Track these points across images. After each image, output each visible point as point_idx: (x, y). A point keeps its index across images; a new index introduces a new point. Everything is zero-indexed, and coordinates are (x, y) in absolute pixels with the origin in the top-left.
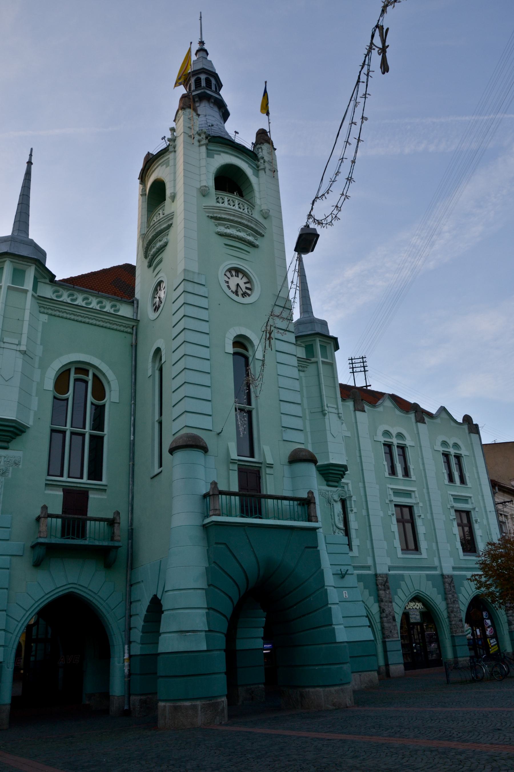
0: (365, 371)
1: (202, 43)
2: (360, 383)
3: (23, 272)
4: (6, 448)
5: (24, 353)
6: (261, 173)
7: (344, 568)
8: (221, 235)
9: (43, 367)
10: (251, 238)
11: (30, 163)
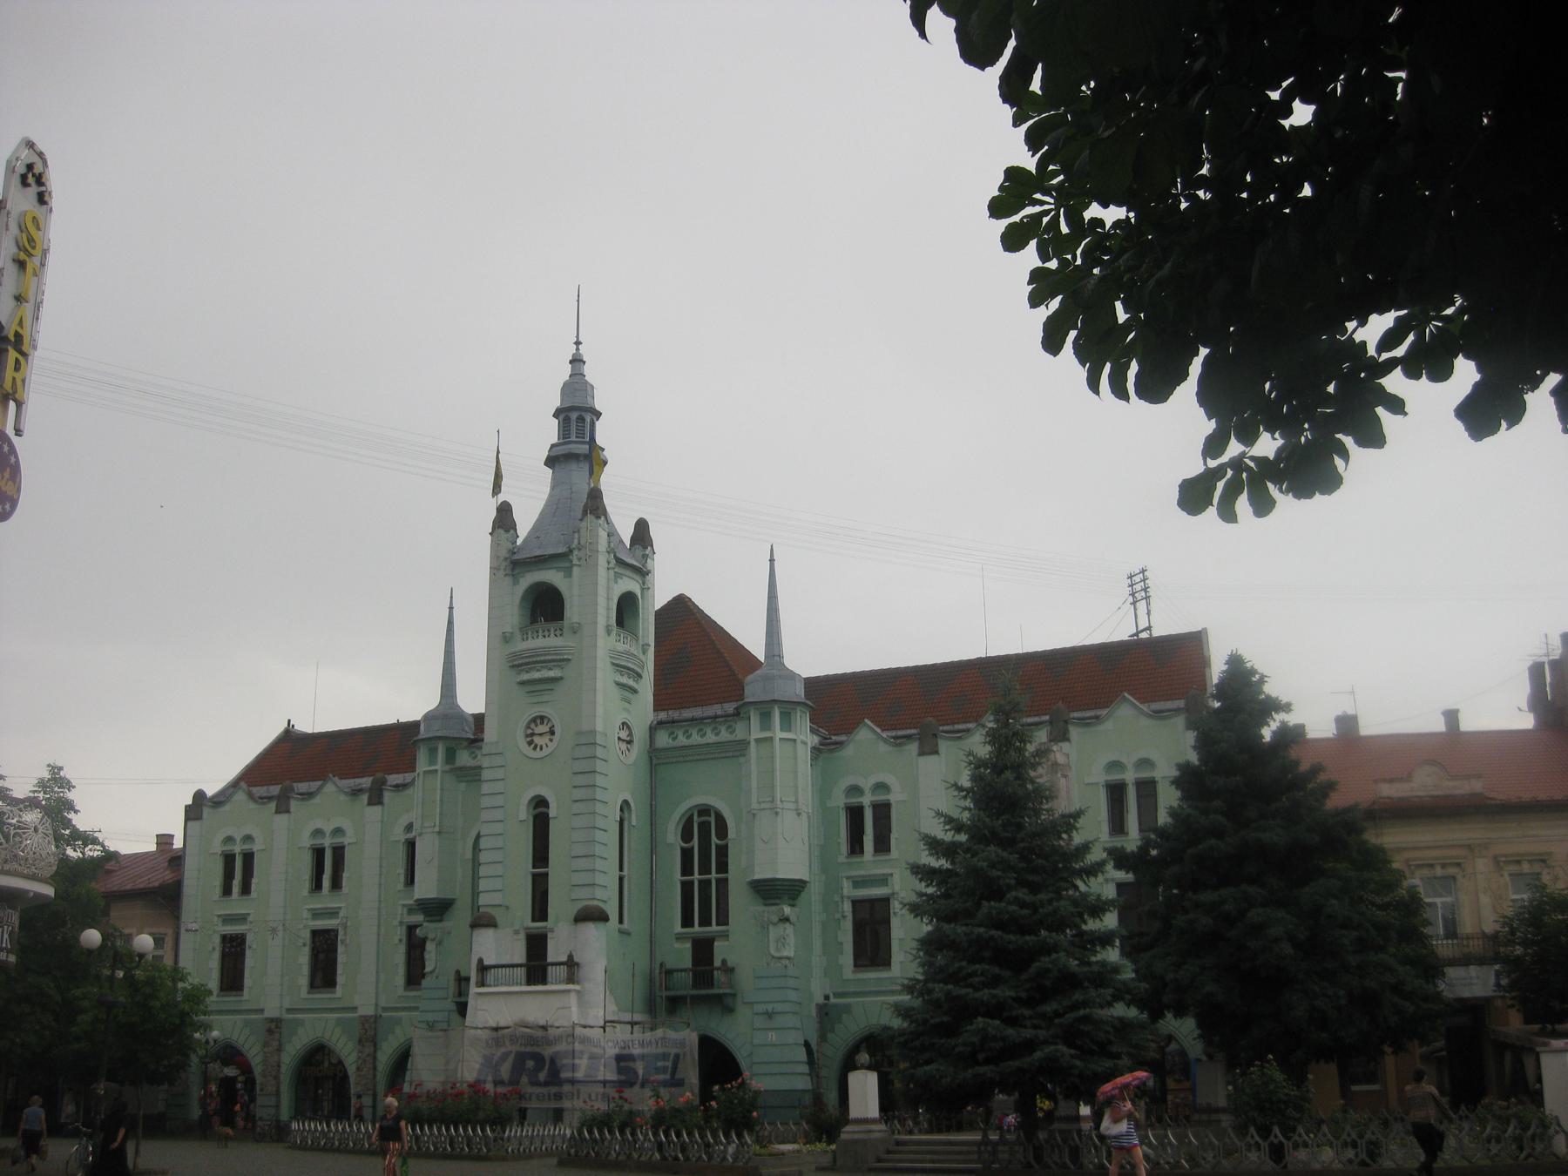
0: (1147, 598)
1: (578, 343)
2: (1143, 624)
3: (436, 749)
6: (575, 570)
8: (522, 683)
10: (551, 674)
11: (451, 608)
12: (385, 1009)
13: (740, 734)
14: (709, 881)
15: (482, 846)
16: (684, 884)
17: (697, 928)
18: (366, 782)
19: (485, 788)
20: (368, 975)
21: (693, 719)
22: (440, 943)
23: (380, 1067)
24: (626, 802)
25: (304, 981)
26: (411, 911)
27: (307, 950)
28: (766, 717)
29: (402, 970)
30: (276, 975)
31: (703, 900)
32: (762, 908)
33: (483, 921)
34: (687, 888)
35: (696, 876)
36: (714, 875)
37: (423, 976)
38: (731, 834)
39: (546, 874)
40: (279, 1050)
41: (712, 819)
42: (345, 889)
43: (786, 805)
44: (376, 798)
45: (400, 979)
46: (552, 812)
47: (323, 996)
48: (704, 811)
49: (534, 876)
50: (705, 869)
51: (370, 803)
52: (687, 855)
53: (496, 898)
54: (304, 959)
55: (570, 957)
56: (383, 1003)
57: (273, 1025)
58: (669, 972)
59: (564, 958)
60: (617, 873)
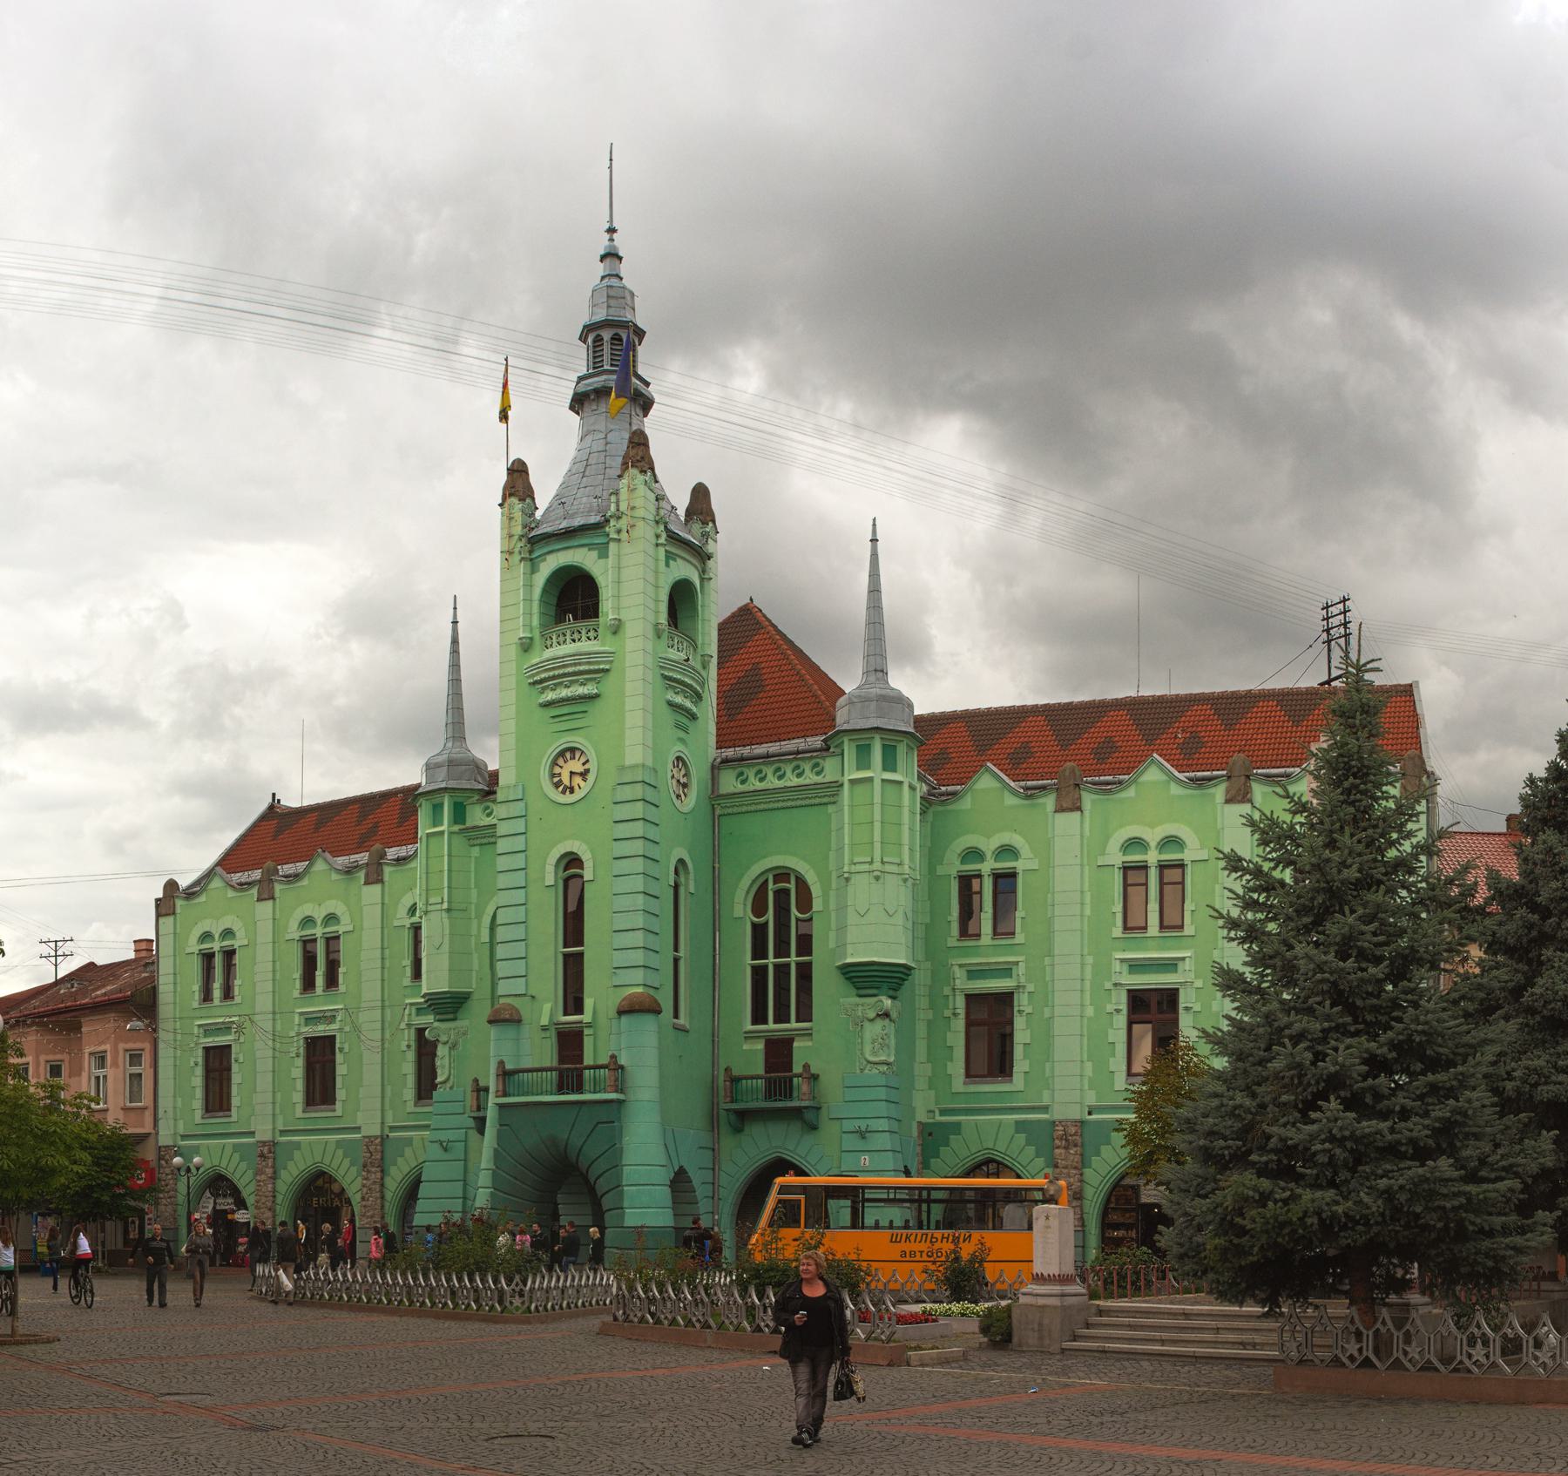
3: (442, 805)
4: (455, 1019)
5: (449, 910)
7: (863, 1125)
9: (479, 917)
12: (392, 1128)
13: (829, 775)
14: (788, 965)
15: (499, 921)
16: (755, 969)
17: (771, 1026)
18: (363, 857)
19: (503, 845)
20: (372, 1089)
21: (768, 756)
22: (454, 1047)
23: (389, 1195)
24: (681, 861)
25: (298, 1097)
26: (419, 1011)
27: (300, 1062)
28: (863, 752)
29: (411, 1081)
30: (267, 1089)
31: (782, 989)
32: (858, 1000)
33: (505, 1018)
34: (759, 974)
35: (771, 960)
36: (793, 959)
37: (434, 1087)
38: (817, 905)
39: (581, 955)
40: (274, 1177)
41: (792, 886)
42: (342, 988)
43: (888, 868)
44: (375, 876)
45: (409, 1093)
46: (588, 874)
47: (320, 1113)
48: (782, 875)
49: (566, 956)
50: (782, 951)
51: (367, 883)
52: (759, 931)
53: (518, 986)
54: (298, 1070)
55: (613, 1057)
56: (390, 1122)
57: (266, 1150)
58: (734, 1080)
59: (604, 1060)
60: (671, 954)
